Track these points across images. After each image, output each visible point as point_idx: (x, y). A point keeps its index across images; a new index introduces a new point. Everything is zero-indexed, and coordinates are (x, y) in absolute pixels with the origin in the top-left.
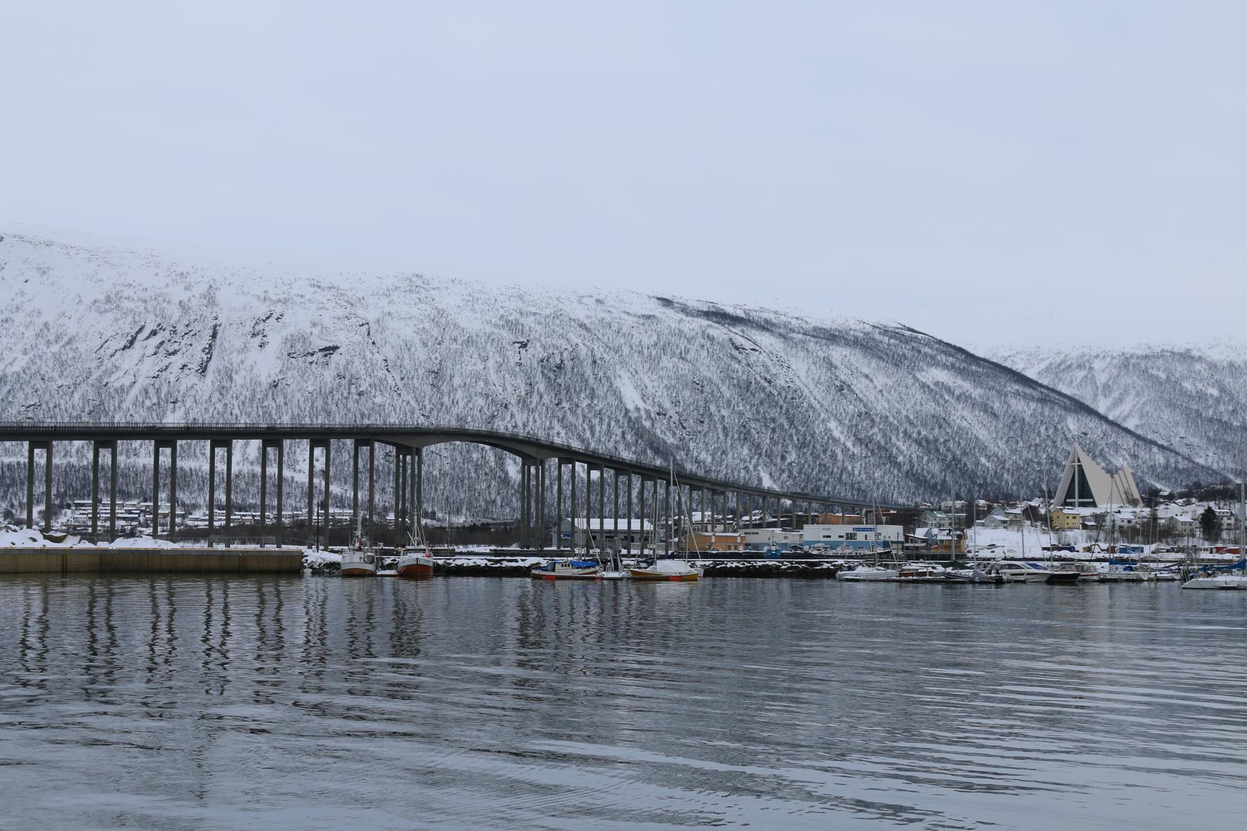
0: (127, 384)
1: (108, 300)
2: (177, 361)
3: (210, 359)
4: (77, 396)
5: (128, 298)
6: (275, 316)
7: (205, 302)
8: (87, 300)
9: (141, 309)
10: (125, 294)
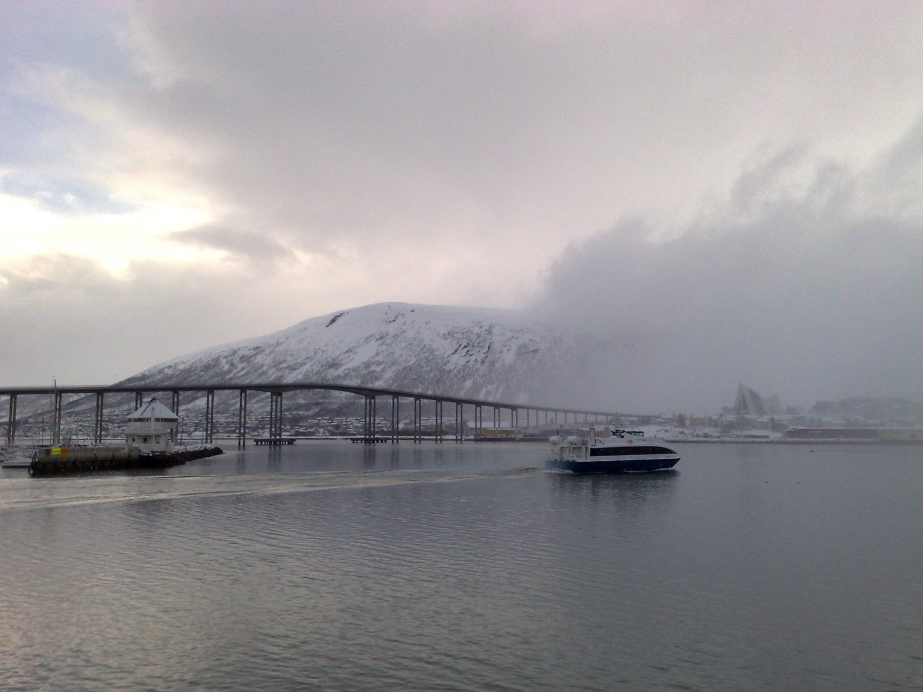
0: (452, 368)
1: (449, 333)
2: (473, 358)
3: (487, 357)
4: (432, 375)
5: (457, 333)
6: (515, 337)
7: (487, 332)
8: (441, 334)
9: (461, 337)
10: (456, 331)
